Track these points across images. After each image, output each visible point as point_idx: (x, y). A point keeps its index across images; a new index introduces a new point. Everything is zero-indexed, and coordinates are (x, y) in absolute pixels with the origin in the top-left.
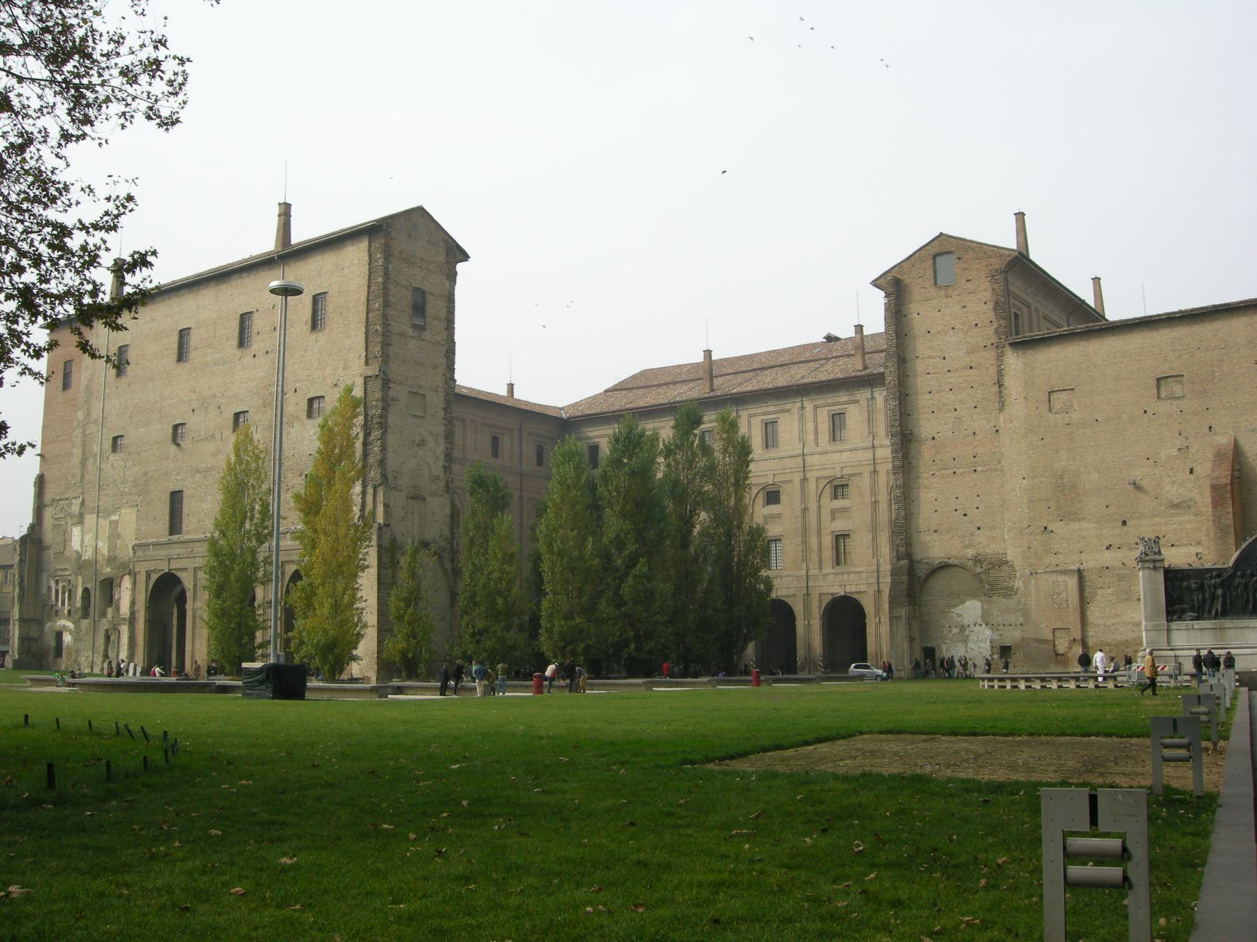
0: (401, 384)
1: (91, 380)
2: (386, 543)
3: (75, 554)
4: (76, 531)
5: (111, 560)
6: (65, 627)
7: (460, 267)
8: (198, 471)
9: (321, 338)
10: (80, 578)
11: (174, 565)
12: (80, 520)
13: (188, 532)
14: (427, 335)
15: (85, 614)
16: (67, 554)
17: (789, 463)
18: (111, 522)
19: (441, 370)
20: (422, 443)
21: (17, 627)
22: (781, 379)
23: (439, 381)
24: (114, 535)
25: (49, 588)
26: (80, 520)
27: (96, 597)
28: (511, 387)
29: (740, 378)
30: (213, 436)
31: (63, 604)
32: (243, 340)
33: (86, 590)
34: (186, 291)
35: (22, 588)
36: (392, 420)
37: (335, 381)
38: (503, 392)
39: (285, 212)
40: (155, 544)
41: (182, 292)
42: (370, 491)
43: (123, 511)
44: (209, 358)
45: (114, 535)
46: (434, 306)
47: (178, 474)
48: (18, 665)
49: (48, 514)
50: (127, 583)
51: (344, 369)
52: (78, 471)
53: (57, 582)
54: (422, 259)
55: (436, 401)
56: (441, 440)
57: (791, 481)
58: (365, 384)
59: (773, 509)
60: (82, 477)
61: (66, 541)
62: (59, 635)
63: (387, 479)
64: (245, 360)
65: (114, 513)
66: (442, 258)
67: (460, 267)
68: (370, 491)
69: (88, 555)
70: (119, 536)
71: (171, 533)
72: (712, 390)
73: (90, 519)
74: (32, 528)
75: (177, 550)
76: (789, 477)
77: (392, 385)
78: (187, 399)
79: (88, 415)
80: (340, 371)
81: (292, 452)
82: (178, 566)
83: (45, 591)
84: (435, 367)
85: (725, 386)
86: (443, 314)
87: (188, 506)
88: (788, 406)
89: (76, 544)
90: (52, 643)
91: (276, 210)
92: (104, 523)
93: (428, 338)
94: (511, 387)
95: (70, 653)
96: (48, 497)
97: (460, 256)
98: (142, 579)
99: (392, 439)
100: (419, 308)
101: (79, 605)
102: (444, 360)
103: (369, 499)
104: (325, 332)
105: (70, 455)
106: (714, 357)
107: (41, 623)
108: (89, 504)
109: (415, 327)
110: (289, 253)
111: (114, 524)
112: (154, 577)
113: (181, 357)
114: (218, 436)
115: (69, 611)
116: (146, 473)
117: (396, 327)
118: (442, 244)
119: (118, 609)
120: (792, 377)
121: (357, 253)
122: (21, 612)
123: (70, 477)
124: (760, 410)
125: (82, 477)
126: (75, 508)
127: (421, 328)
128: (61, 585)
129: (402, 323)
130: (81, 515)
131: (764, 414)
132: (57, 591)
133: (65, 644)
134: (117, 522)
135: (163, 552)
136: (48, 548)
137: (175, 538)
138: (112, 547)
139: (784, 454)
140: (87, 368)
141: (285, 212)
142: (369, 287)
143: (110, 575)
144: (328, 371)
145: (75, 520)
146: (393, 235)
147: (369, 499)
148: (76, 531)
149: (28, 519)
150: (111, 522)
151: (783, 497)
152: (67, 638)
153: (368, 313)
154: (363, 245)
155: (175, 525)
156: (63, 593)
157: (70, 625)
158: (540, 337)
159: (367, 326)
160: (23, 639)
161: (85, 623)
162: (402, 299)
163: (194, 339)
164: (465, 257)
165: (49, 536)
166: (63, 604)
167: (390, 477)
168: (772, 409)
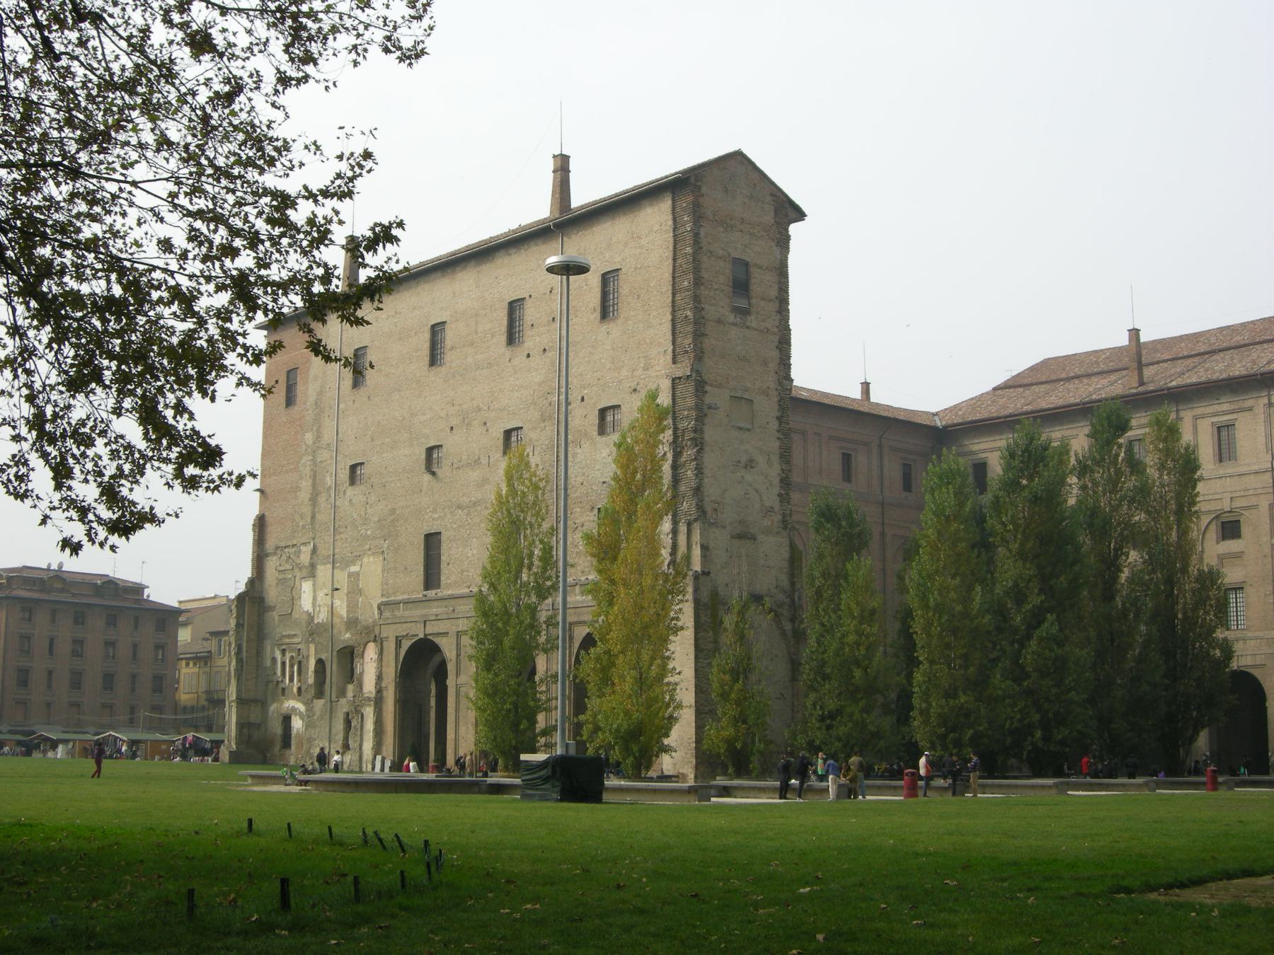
0: (720, 386)
1: (320, 393)
2: (705, 596)
3: (305, 617)
4: (307, 586)
5: (352, 623)
6: (294, 709)
7: (794, 229)
8: (459, 507)
9: (614, 329)
10: (312, 647)
11: (429, 630)
13: (449, 586)
14: (752, 320)
15: (320, 694)
16: (295, 615)
17: (1252, 482)
18: (350, 575)
19: (773, 366)
20: (750, 464)
21: (234, 710)
22: (1239, 366)
23: (770, 381)
25: (274, 660)
26: (312, 572)
27: (333, 670)
28: (866, 387)
29: (1180, 366)
30: (477, 461)
31: (291, 680)
32: (513, 337)
33: (320, 662)
34: (439, 274)
35: (239, 660)
36: (710, 434)
37: (633, 385)
38: (856, 394)
39: (562, 165)
40: (406, 602)
41: (433, 276)
42: (683, 528)
43: (365, 560)
44: (470, 360)
45: (355, 591)
46: (761, 283)
47: (435, 511)
48: (236, 758)
49: (271, 564)
50: (371, 652)
51: (645, 369)
52: (307, 510)
53: (283, 651)
54: (743, 221)
55: (767, 408)
56: (775, 459)
57: (1256, 507)
58: (674, 388)
59: (1231, 546)
60: (313, 517)
61: (293, 600)
62: (287, 720)
63: (704, 512)
64: (516, 362)
65: (353, 562)
66: (769, 218)
67: (794, 229)
68: (683, 528)
69: (322, 617)
70: (360, 592)
72: (1142, 383)
73: (323, 571)
74: (251, 582)
75: (435, 610)
76: (1253, 501)
77: (708, 388)
78: (443, 414)
80: (640, 371)
81: (580, 479)
82: (436, 630)
83: (268, 663)
84: (765, 363)
85: (1157, 378)
86: (774, 293)
87: (448, 552)
88: (1249, 403)
89: (306, 603)
90: (278, 730)
91: (550, 165)
92: (342, 578)
93: (754, 325)
94: (866, 387)
95: (300, 744)
96: (270, 545)
97: (792, 214)
98: (390, 647)
99: (710, 460)
100: (741, 286)
101: (311, 680)
102: (775, 354)
103: (682, 539)
104: (620, 321)
105: (298, 489)
106: (1143, 339)
107: (264, 704)
108: (322, 551)
109: (737, 310)
110: (568, 220)
112: (406, 644)
113: (434, 360)
114: (484, 461)
115: (299, 689)
116: (393, 511)
117: (711, 311)
118: (768, 199)
119: (360, 686)
120: (1254, 362)
121: (658, 216)
122: (238, 691)
123: (297, 518)
124: (1209, 410)
125: (313, 517)
126: (305, 558)
127: (745, 312)
128: (288, 655)
129: (719, 305)
130: (313, 566)
131: (1215, 415)
132: (283, 664)
133: (294, 732)
134: (357, 574)
135: (416, 613)
136: (272, 608)
137: (431, 593)
138: (352, 606)
139: (1244, 469)
140: (316, 377)
141: (562, 165)
142: (674, 259)
143: (351, 643)
144: (624, 373)
145: (305, 572)
146: (704, 190)
147: (682, 539)
148: (307, 586)
149: (246, 572)
150: (350, 575)
151: (1245, 530)
152: (297, 724)
153: (674, 294)
154: (665, 205)
155: (431, 577)
156: (292, 666)
157: (301, 707)
158: (902, 321)
159: (674, 312)
160: (241, 725)
161: (319, 704)
162: (719, 275)
163: (450, 337)
164: (800, 215)
165: (272, 593)
166: (291, 680)
167: (709, 509)
168: (1226, 407)
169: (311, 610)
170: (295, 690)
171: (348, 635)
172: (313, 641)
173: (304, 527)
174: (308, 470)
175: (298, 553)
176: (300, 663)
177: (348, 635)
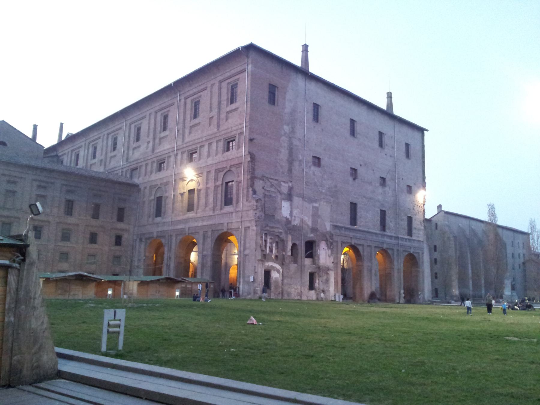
1: (293, 112)
3: (285, 220)
8: (364, 197)
10: (290, 237)
12: (289, 197)
13: (360, 226)
16: (277, 217)
18: (313, 207)
24: (316, 215)
27: (302, 249)
33: (294, 246)
34: (353, 101)
41: (350, 99)
43: (322, 203)
52: (285, 165)
53: (266, 234)
65: (315, 201)
70: (319, 217)
71: (351, 224)
79: (293, 131)
82: (359, 243)
87: (360, 212)
111: (316, 209)
115: (276, 256)
116: (336, 186)
125: (290, 170)
128: (269, 237)
134: (317, 208)
138: (314, 221)
143: (314, 239)
150: (313, 207)
152: (275, 275)
155: (354, 220)
157: (278, 266)
169: (288, 217)
170: (273, 257)
171: (312, 235)
172: (290, 233)
173: (283, 173)
174: (286, 145)
175: (280, 186)
176: (277, 243)
177: (312, 235)
